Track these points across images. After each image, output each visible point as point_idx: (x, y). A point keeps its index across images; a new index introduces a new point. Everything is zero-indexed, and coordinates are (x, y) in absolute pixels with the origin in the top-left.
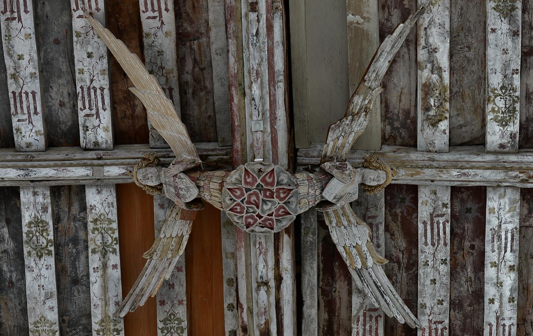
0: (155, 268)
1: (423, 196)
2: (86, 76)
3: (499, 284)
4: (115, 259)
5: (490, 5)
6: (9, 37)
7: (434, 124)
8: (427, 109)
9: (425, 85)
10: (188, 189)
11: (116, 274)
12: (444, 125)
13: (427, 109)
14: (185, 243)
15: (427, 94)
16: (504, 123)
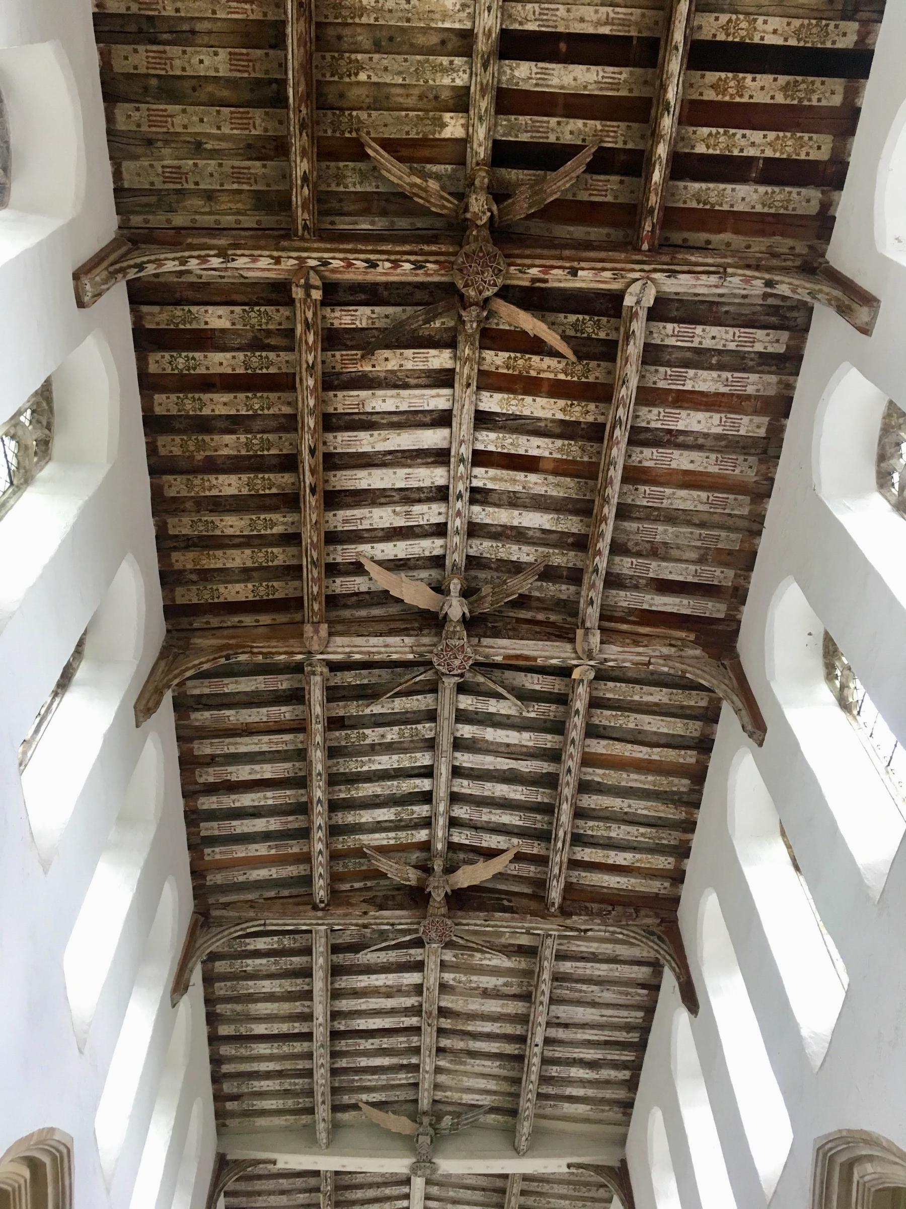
0: (391, 866)
1: (420, 951)
2: (488, 839)
3: (377, 980)
4: (392, 842)
5: (510, 980)
6: (512, 814)
7: (454, 956)
8: (462, 954)
9: (473, 955)
10: (439, 895)
11: (385, 842)
12: (454, 959)
13: (462, 954)
14: (408, 883)
15: (470, 955)
16: (454, 979)
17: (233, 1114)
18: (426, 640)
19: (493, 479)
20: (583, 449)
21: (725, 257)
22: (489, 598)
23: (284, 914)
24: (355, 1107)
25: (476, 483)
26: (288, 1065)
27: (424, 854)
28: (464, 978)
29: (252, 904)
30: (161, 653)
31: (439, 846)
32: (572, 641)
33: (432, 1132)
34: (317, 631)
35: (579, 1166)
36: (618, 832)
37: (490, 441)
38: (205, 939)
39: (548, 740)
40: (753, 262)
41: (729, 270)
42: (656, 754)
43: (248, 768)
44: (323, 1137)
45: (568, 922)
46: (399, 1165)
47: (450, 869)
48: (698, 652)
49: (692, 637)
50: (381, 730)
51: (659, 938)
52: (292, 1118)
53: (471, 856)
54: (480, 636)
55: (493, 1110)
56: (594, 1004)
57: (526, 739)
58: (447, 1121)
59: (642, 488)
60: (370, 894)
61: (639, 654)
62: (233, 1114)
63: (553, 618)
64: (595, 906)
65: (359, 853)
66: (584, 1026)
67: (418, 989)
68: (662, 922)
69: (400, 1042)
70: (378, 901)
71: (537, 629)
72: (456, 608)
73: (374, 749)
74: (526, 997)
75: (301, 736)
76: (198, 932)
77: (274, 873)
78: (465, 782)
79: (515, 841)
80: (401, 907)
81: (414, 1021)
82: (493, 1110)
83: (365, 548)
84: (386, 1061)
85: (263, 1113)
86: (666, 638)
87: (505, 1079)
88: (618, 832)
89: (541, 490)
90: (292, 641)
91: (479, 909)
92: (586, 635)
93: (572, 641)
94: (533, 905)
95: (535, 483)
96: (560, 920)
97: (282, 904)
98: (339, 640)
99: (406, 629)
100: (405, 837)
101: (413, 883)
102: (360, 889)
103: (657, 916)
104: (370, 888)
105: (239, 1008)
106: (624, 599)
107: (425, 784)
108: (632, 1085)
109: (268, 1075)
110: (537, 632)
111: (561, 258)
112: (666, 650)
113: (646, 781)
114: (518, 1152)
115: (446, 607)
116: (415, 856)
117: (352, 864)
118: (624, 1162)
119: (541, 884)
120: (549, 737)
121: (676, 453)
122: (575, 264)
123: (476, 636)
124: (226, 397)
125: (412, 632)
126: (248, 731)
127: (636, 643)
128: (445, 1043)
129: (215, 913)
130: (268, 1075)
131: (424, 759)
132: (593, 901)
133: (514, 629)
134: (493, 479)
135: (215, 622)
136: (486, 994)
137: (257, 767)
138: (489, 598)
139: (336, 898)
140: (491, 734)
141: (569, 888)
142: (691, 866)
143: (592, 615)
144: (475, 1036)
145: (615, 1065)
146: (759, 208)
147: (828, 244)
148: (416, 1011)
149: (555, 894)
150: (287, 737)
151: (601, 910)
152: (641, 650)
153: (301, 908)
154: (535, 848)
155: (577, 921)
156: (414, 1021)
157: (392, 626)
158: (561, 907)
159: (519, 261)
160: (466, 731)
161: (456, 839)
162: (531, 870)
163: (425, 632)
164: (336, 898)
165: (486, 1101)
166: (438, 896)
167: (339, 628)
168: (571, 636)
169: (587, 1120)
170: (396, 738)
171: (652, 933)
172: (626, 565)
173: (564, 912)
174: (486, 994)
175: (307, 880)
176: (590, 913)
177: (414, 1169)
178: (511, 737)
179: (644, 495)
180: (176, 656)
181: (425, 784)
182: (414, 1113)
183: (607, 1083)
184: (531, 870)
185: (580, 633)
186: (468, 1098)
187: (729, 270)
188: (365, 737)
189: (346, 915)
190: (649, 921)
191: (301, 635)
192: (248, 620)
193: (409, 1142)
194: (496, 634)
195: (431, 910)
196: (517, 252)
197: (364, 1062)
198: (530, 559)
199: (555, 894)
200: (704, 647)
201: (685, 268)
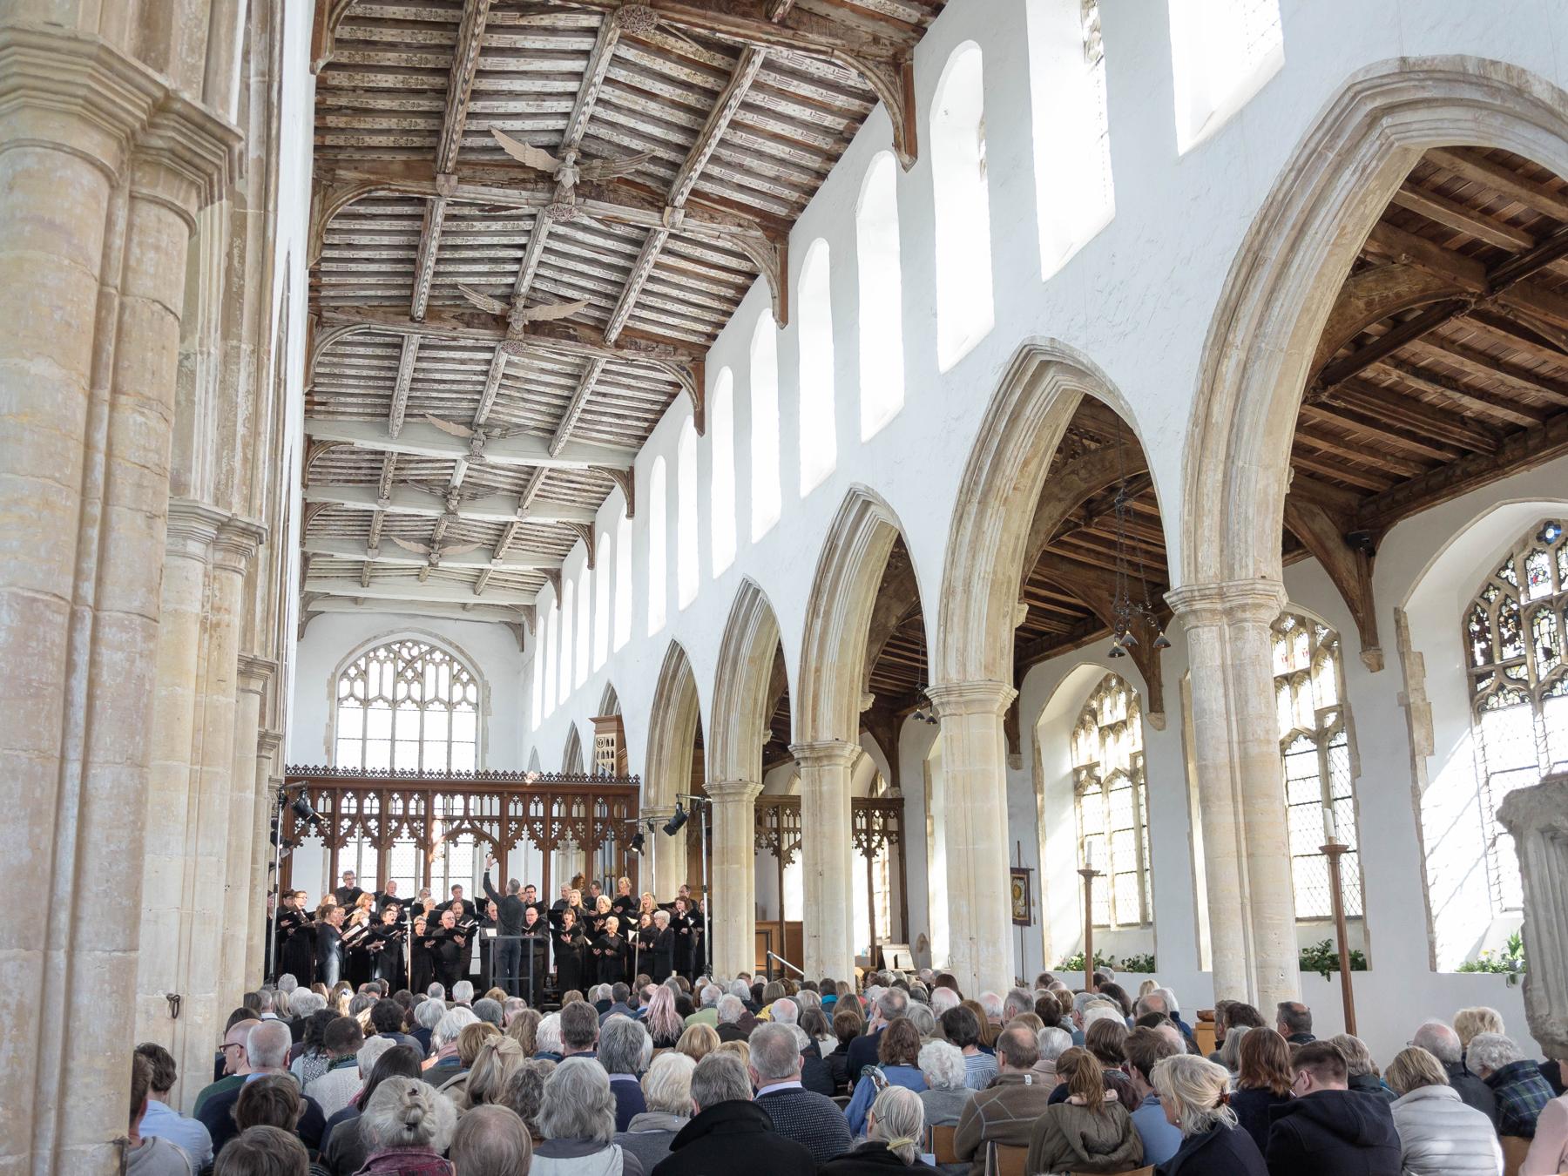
17: (319, 412)
18: (540, 195)
19: (619, 97)
20: (698, 101)
21: (836, 36)
22: (598, 171)
23: (386, 322)
24: (423, 416)
25: (602, 96)
26: (372, 392)
27: (509, 290)
28: (527, 360)
29: (358, 311)
30: (314, 187)
31: (523, 290)
32: (661, 210)
33: (484, 438)
34: (448, 181)
35: (598, 468)
36: (669, 306)
37: (621, 74)
38: (322, 338)
39: (628, 249)
40: (856, 47)
41: (836, 52)
42: (713, 273)
43: (369, 237)
44: (396, 434)
45: (620, 353)
46: (458, 454)
47: (531, 302)
48: (759, 233)
49: (757, 220)
50: (488, 223)
51: (688, 373)
52: (369, 418)
53: (548, 296)
54: (585, 196)
55: (536, 428)
56: (629, 387)
57: (610, 244)
58: (497, 431)
59: (739, 133)
60: (460, 311)
61: (713, 229)
62: (319, 412)
63: (648, 184)
64: (643, 343)
65: (455, 286)
66: (617, 397)
67: (489, 362)
68: (693, 359)
69: (469, 387)
70: (466, 318)
71: (634, 192)
72: (569, 177)
73: (479, 233)
74: (577, 377)
75: (418, 223)
76: (315, 330)
77: (379, 293)
78: (553, 258)
79: (587, 296)
80: (485, 326)
81: (482, 378)
82: (536, 428)
83: (499, 124)
84: (454, 396)
85: (343, 413)
86: (736, 216)
87: (549, 414)
88: (669, 306)
89: (658, 114)
90: (425, 183)
91: (549, 335)
92: (673, 212)
93: (661, 210)
94: (594, 336)
95: (653, 108)
96: (614, 351)
97: (385, 313)
98: (466, 187)
99: (524, 181)
100: (493, 280)
101: (497, 312)
102: (450, 306)
103: (690, 354)
104: (459, 306)
105: (335, 360)
106: (707, 187)
107: (519, 254)
108: (650, 430)
109: (352, 395)
110: (634, 197)
111: (705, 18)
112: (735, 229)
113: (704, 286)
114: (549, 452)
115: (560, 177)
116: (499, 292)
117: (445, 292)
118: (632, 469)
119: (601, 327)
120: (629, 247)
121: (772, 122)
122: (716, 26)
123: (584, 196)
124: (394, 31)
125: (530, 186)
126: (374, 217)
127: (712, 218)
128: (502, 391)
129: (326, 314)
130: (352, 395)
131: (522, 240)
132: (642, 338)
133: (615, 191)
134: (619, 97)
135: (357, 156)
136: (543, 371)
137: (377, 238)
138: (598, 171)
139: (432, 313)
140: (580, 235)
141: (626, 327)
142: (722, 333)
143: (680, 200)
144: (528, 391)
145: (638, 419)
146: (872, 8)
147: (919, 40)
148: (486, 373)
149: (614, 336)
150: (405, 223)
151: (648, 346)
152: (714, 225)
153: (401, 318)
154: (603, 303)
155: (626, 353)
156: (482, 378)
157: (512, 175)
158: (616, 341)
159: (670, 14)
160: (561, 230)
161: (537, 285)
162: (597, 314)
163: (540, 186)
164: (432, 313)
165: (533, 424)
166: (518, 323)
167: (466, 172)
168: (661, 204)
169: (609, 442)
170: (499, 228)
171: (683, 369)
172: (716, 171)
173: (618, 345)
174: (543, 371)
175: (410, 298)
176: (638, 349)
177: (466, 459)
178: (600, 241)
179: (740, 138)
180: (326, 188)
181: (519, 254)
182: (470, 424)
183: (629, 427)
184: (597, 314)
185: (668, 209)
186: (515, 420)
187: (836, 52)
188: (473, 226)
189: (439, 328)
190: (684, 358)
191: (434, 179)
192: (386, 157)
193: (468, 442)
194: (599, 197)
195: (510, 335)
196: (670, 5)
197: (435, 395)
198: (640, 148)
199: (614, 336)
200: (765, 229)
201: (802, 44)
